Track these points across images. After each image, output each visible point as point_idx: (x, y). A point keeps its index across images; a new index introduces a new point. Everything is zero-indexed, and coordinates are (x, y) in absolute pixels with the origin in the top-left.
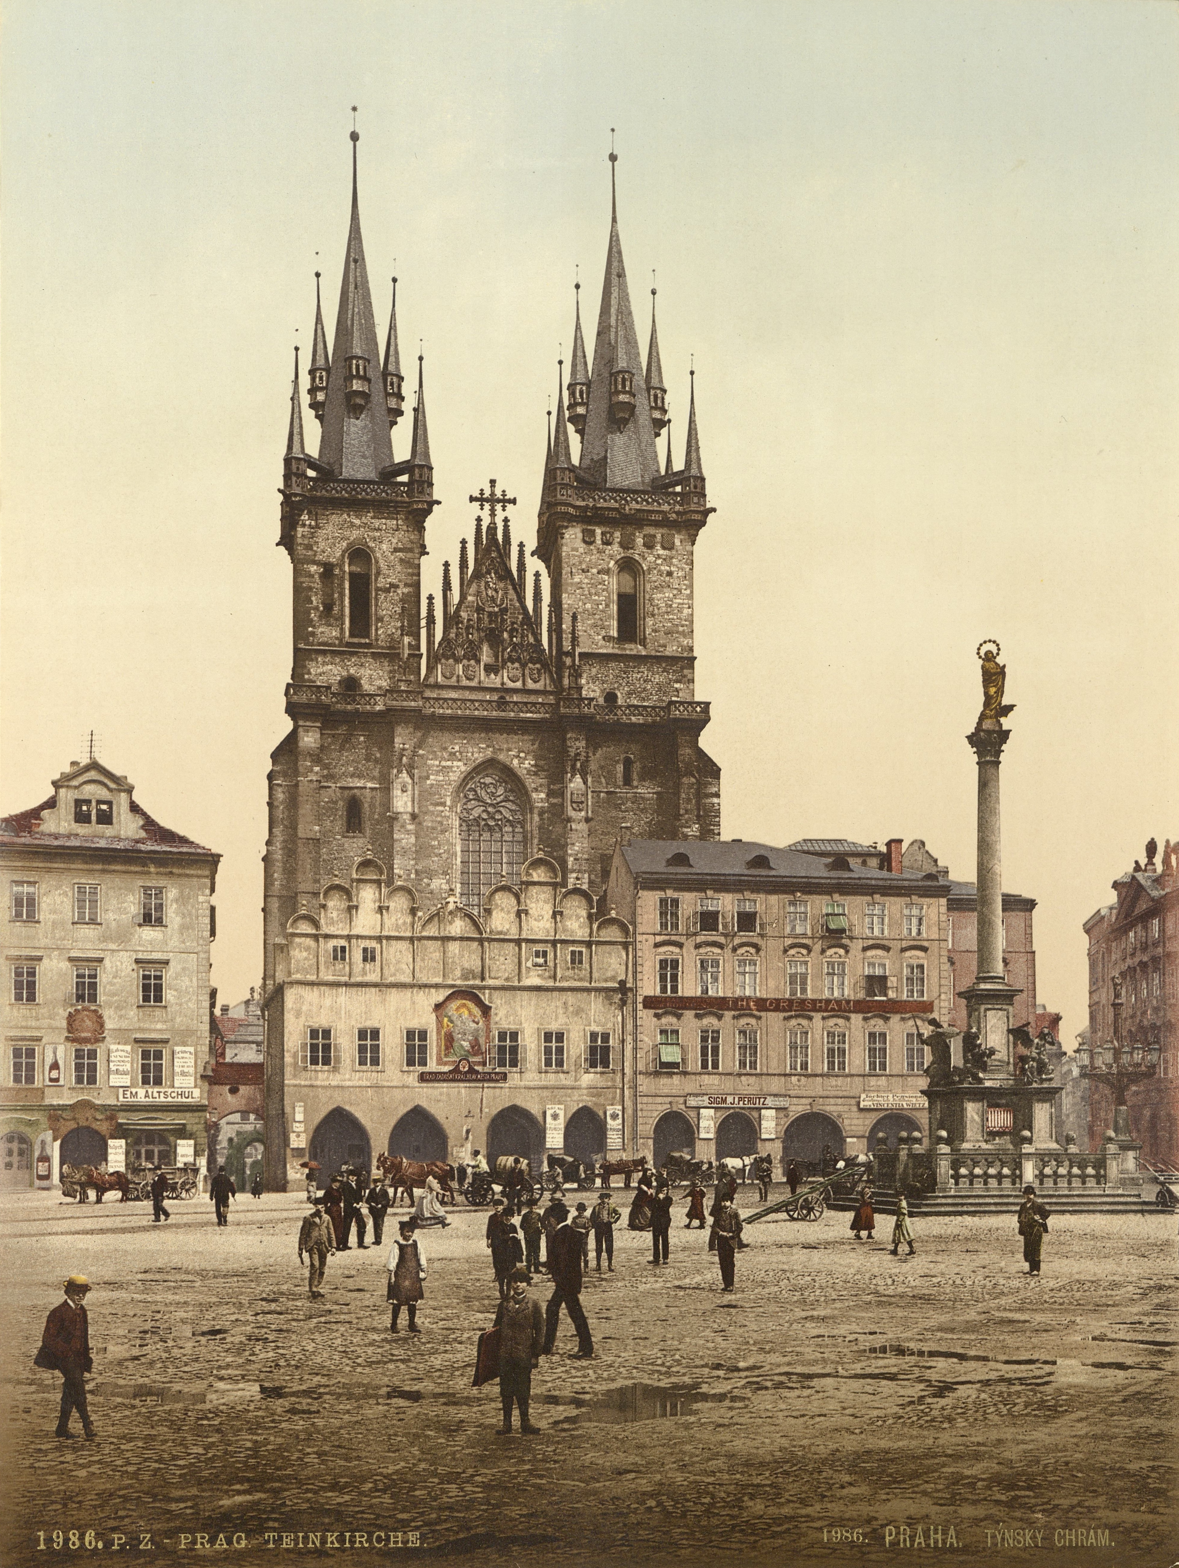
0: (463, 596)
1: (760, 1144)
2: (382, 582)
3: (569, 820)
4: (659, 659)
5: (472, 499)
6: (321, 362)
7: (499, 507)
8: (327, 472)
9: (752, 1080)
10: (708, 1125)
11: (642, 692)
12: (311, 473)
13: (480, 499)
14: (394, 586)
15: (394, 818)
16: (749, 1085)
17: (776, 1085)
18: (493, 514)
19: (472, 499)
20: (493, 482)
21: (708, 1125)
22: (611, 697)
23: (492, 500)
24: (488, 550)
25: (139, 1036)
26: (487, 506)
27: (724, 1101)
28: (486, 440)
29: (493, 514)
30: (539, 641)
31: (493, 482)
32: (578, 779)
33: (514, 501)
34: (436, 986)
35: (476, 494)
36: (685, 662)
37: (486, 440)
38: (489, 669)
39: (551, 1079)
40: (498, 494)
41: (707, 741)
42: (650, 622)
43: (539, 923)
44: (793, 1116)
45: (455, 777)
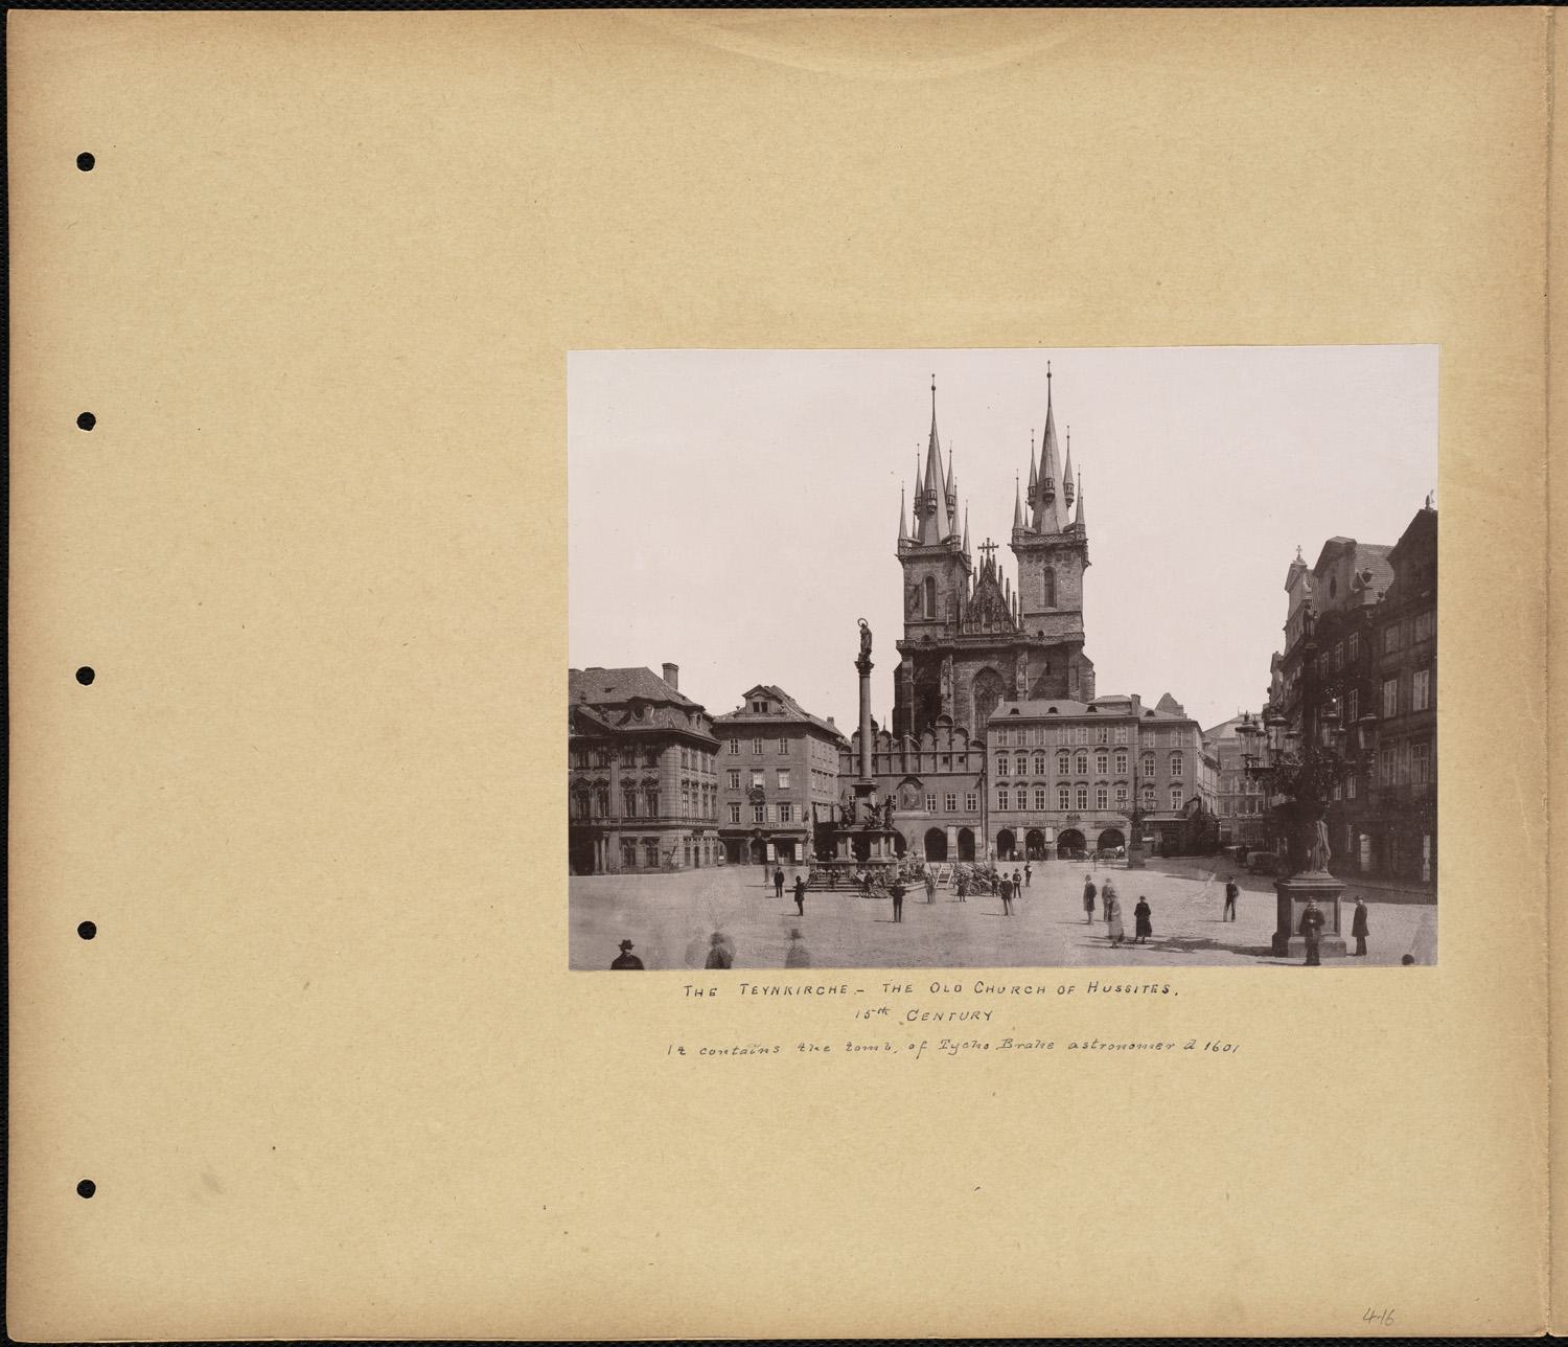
0: (975, 594)
1: (1016, 844)
2: (939, 591)
3: (1018, 692)
4: (1062, 614)
5: (979, 548)
6: (919, 495)
7: (991, 551)
8: (917, 545)
9: (1042, 814)
10: (1021, 835)
11: (1054, 631)
13: (983, 548)
14: (944, 592)
15: (942, 697)
16: (1041, 816)
17: (1054, 816)
19: (979, 548)
20: (988, 539)
21: (1021, 835)
22: (1041, 633)
23: (988, 547)
24: (985, 571)
25: (779, 801)
27: (1028, 823)
28: (988, 523)
30: (1008, 610)
31: (988, 539)
32: (1021, 673)
33: (997, 547)
34: (900, 775)
35: (981, 545)
36: (1077, 613)
37: (988, 523)
38: (986, 626)
39: (950, 815)
41: (1086, 651)
42: (1058, 596)
43: (943, 746)
44: (1061, 830)
45: (971, 676)
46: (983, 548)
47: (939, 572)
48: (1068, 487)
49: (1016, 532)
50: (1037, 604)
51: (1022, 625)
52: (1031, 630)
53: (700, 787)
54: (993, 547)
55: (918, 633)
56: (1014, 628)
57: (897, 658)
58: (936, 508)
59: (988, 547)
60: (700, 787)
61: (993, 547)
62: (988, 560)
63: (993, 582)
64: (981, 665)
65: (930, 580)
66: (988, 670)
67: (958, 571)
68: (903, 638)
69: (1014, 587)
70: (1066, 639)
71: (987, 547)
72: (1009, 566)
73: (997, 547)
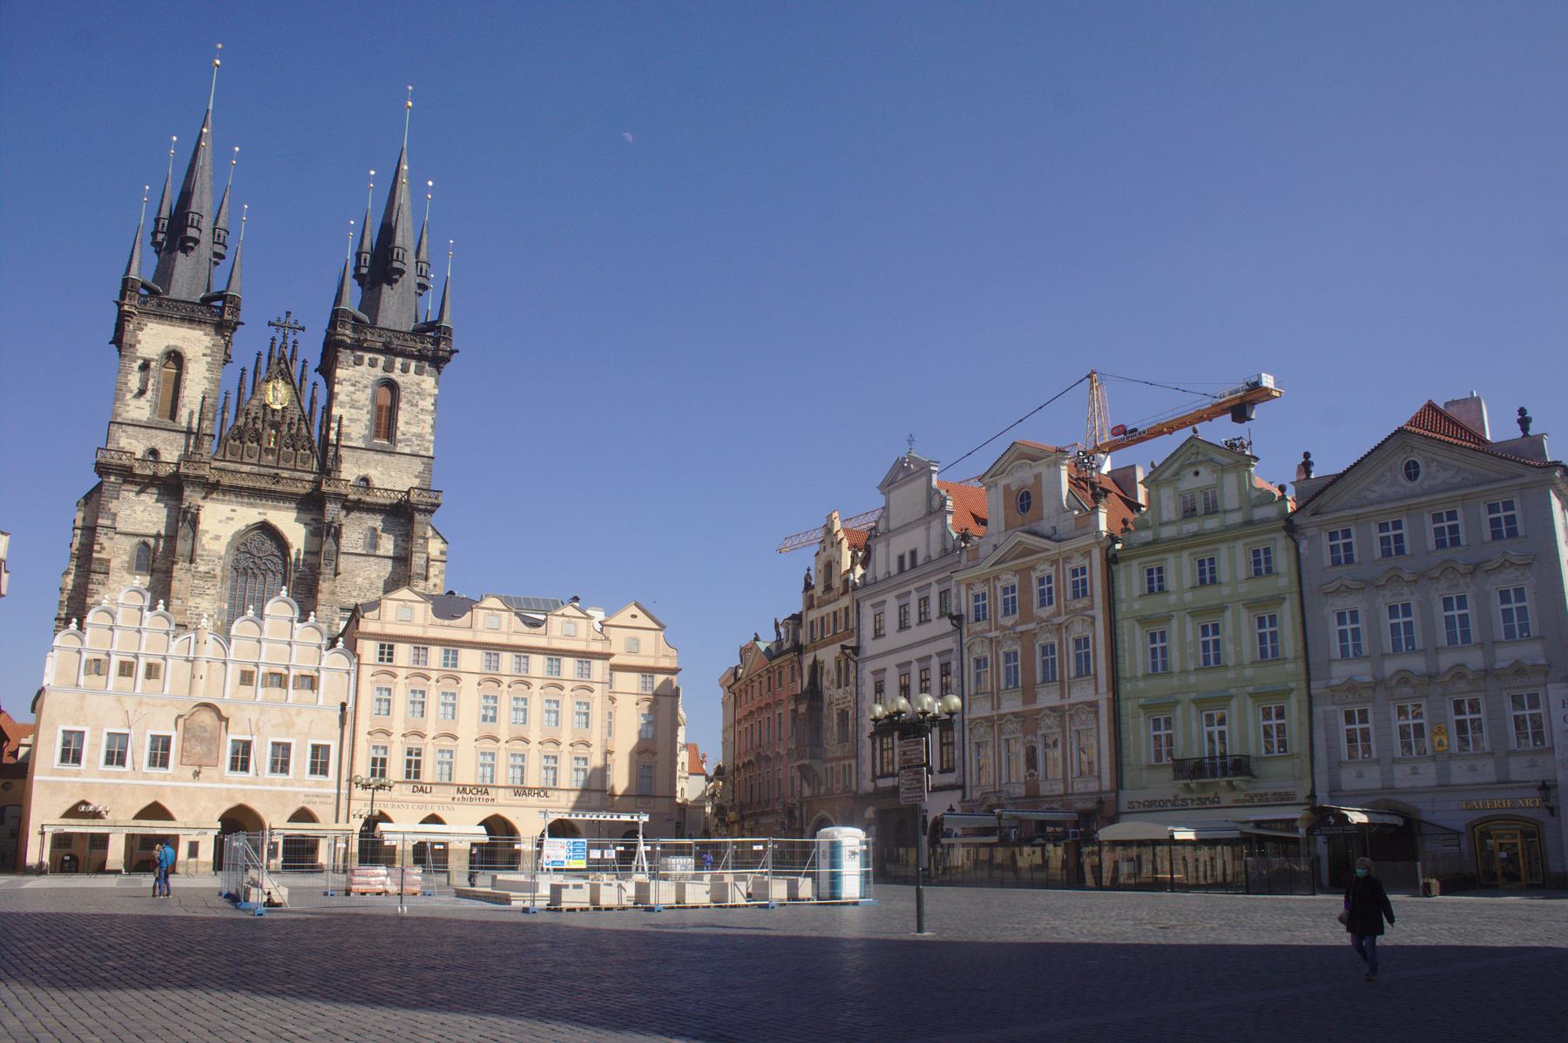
20: (288, 313)
29: (285, 336)
31: (288, 313)
35: (274, 320)
58: (197, 241)
59: (286, 325)
64: (249, 514)
65: (175, 358)
66: (266, 528)
70: (414, 498)
73: (303, 329)
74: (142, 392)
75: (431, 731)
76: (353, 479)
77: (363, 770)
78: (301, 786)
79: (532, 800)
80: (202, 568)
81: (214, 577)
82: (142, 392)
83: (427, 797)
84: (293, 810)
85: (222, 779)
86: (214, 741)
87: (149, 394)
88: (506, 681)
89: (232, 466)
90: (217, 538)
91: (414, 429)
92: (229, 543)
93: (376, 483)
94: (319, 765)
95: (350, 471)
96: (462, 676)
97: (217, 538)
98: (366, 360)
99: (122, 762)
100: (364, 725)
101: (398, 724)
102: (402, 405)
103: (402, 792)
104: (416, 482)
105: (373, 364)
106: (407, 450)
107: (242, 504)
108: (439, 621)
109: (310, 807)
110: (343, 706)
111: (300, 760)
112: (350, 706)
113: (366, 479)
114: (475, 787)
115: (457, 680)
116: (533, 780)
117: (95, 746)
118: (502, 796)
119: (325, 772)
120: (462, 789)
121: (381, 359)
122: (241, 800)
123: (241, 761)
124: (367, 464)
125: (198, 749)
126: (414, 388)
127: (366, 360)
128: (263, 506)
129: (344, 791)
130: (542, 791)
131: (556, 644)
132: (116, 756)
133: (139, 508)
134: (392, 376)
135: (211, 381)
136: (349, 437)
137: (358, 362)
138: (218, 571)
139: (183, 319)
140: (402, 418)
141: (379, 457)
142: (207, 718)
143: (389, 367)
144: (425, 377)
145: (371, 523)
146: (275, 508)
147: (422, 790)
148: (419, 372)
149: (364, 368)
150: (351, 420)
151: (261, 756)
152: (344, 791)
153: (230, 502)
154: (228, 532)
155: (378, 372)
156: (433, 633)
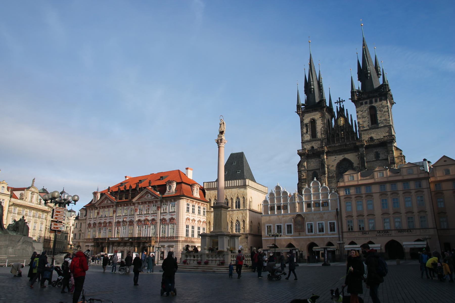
12: (302, 107)
13: (337, 102)
18: (340, 105)
20: (339, 98)
23: (340, 102)
26: (339, 103)
29: (340, 105)
31: (339, 98)
33: (344, 101)
37: (339, 89)
40: (341, 100)
46: (337, 102)
47: (317, 116)
48: (376, 67)
49: (353, 93)
50: (366, 123)
51: (360, 135)
52: (365, 137)
53: (196, 222)
54: (342, 101)
55: (308, 147)
56: (357, 138)
57: (298, 159)
58: (314, 89)
60: (196, 222)
61: (342, 101)
62: (340, 107)
63: (344, 117)
65: (313, 122)
66: (345, 160)
67: (327, 115)
68: (300, 148)
69: (355, 118)
71: (340, 102)
72: (351, 109)
73: (344, 101)
74: (307, 132)
75: (365, 213)
76: (367, 139)
77: (345, 228)
78: (328, 235)
79: (405, 233)
80: (330, 175)
81: (334, 177)
82: (307, 132)
83: (367, 236)
84: (326, 242)
85: (306, 235)
86: (303, 224)
87: (309, 133)
88: (389, 193)
89: (333, 145)
90: (333, 166)
91: (383, 118)
92: (336, 167)
93: (375, 138)
94: (332, 229)
95: (365, 137)
96: (374, 194)
97: (333, 166)
98: (364, 103)
99: (323, 231)
100: (344, 215)
101: (355, 214)
102: (378, 112)
103: (359, 235)
104: (387, 134)
105: (366, 103)
106: (382, 125)
107: (338, 155)
108: (363, 178)
109: (331, 241)
110: (337, 209)
111: (327, 228)
112: (339, 210)
113: (371, 138)
114: (383, 231)
115: (372, 196)
116: (405, 226)
117: (274, 229)
118: (393, 233)
119: (334, 231)
120: (379, 232)
121: (368, 101)
122: (312, 241)
123: (311, 230)
124: (371, 133)
125: (299, 227)
126: (380, 106)
127: (364, 103)
128: (343, 154)
129: (341, 236)
130: (409, 230)
131: (406, 178)
132: (321, 230)
133: (312, 163)
134: (373, 105)
135: (323, 124)
136: (363, 127)
137: (362, 104)
138: (335, 175)
139: (313, 110)
140: (378, 116)
141: (374, 130)
142: (299, 218)
143: (371, 102)
144: (383, 101)
145: (375, 151)
146: (348, 153)
147: (365, 233)
148: (381, 100)
149: (363, 106)
150: (364, 122)
151: (316, 228)
152: (341, 236)
153: (334, 155)
154: (335, 164)
155: (369, 105)
156: (360, 183)
